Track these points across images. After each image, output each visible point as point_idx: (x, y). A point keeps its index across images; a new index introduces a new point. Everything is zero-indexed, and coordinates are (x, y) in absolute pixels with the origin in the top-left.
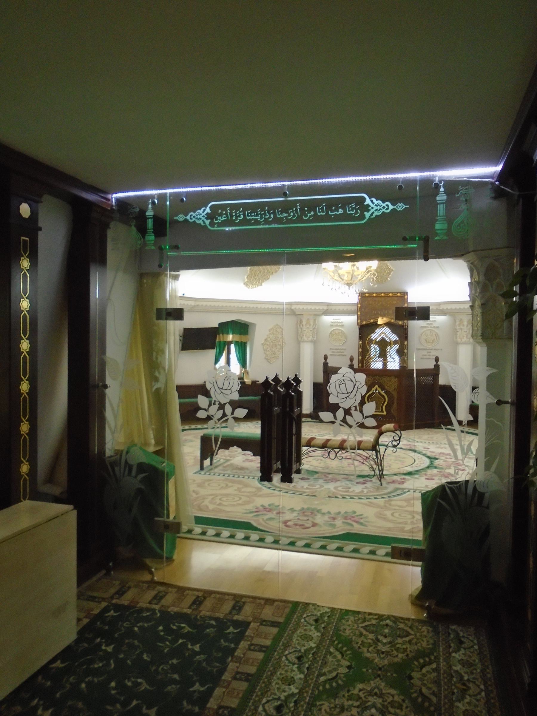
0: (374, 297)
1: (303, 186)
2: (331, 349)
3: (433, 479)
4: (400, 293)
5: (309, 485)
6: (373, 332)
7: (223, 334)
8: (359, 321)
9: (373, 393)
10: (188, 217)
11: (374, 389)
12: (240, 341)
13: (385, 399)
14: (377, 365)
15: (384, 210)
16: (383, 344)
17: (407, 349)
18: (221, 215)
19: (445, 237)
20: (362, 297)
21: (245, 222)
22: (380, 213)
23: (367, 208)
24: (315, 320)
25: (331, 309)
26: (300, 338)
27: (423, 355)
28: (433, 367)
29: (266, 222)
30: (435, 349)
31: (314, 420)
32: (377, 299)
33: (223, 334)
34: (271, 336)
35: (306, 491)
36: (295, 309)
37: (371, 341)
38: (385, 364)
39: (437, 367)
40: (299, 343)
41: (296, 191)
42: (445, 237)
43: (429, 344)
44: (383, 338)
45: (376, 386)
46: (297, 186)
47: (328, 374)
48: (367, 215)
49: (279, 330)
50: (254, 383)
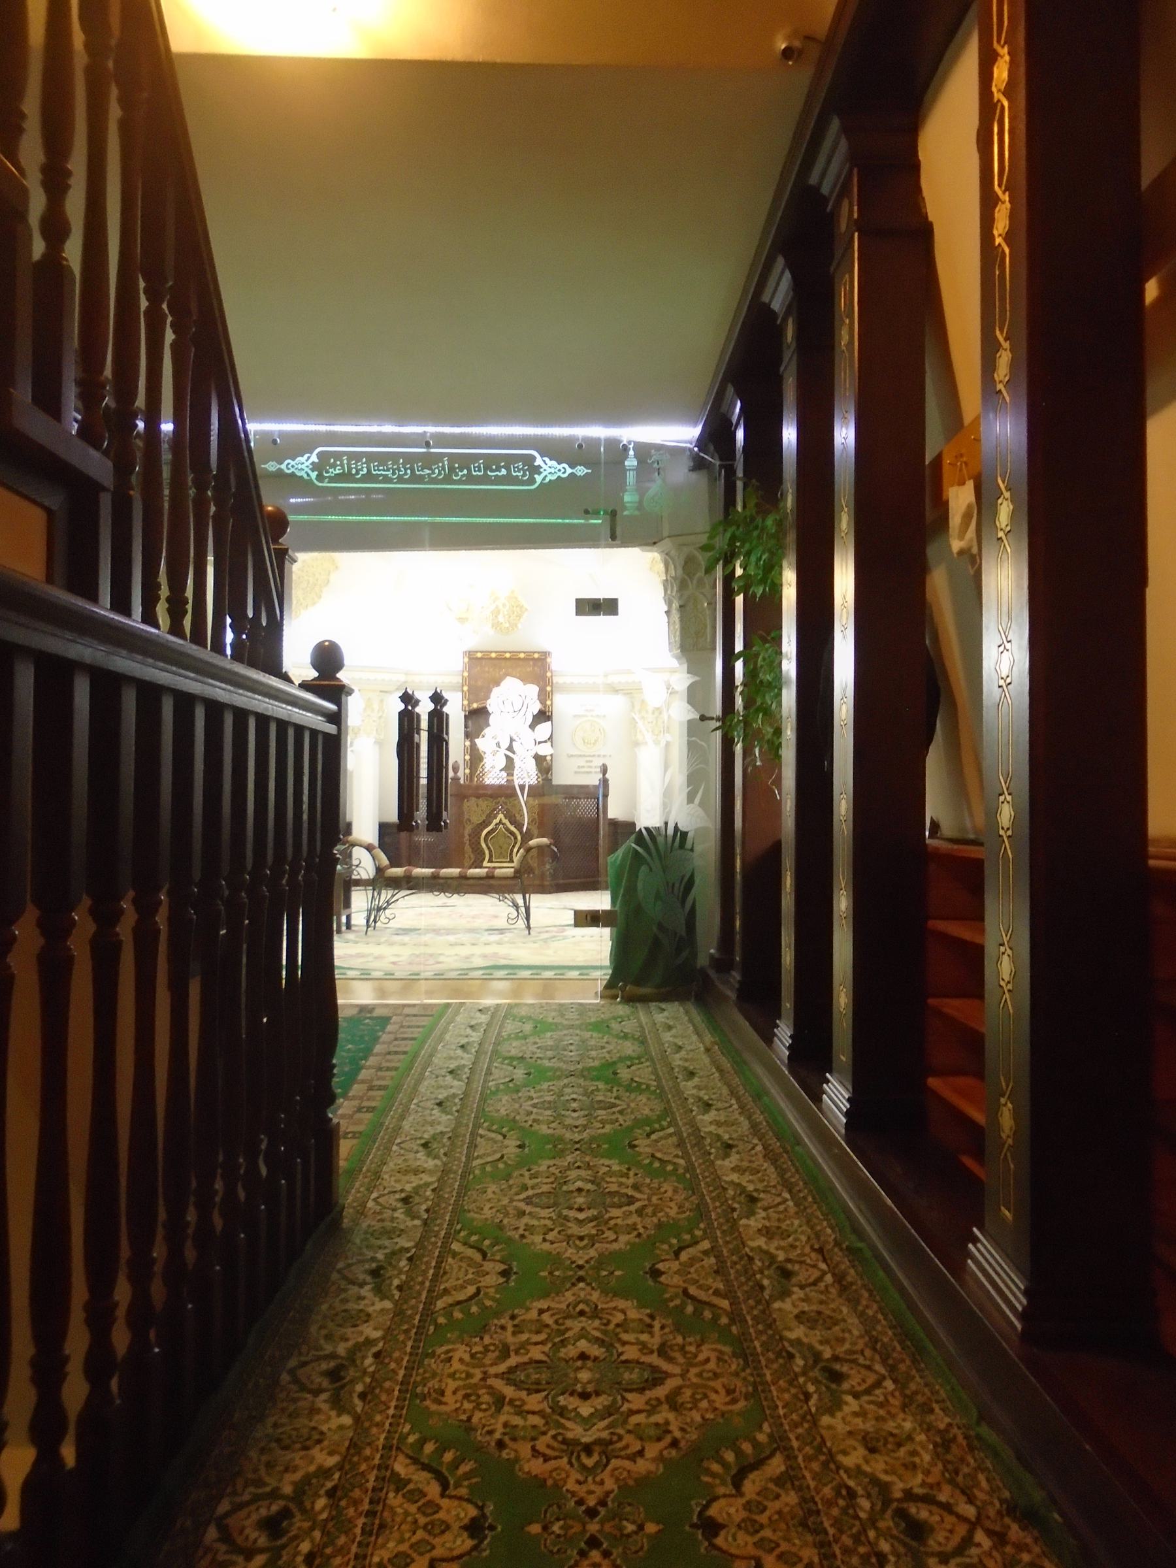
1: (453, 436)
8: (466, 702)
10: (283, 466)
13: (516, 838)
15: (560, 474)
18: (334, 466)
19: (637, 513)
21: (369, 477)
22: (554, 477)
23: (537, 470)
24: (382, 701)
29: (401, 480)
39: (605, 782)
41: (443, 440)
42: (637, 513)
46: (443, 435)
48: (538, 478)
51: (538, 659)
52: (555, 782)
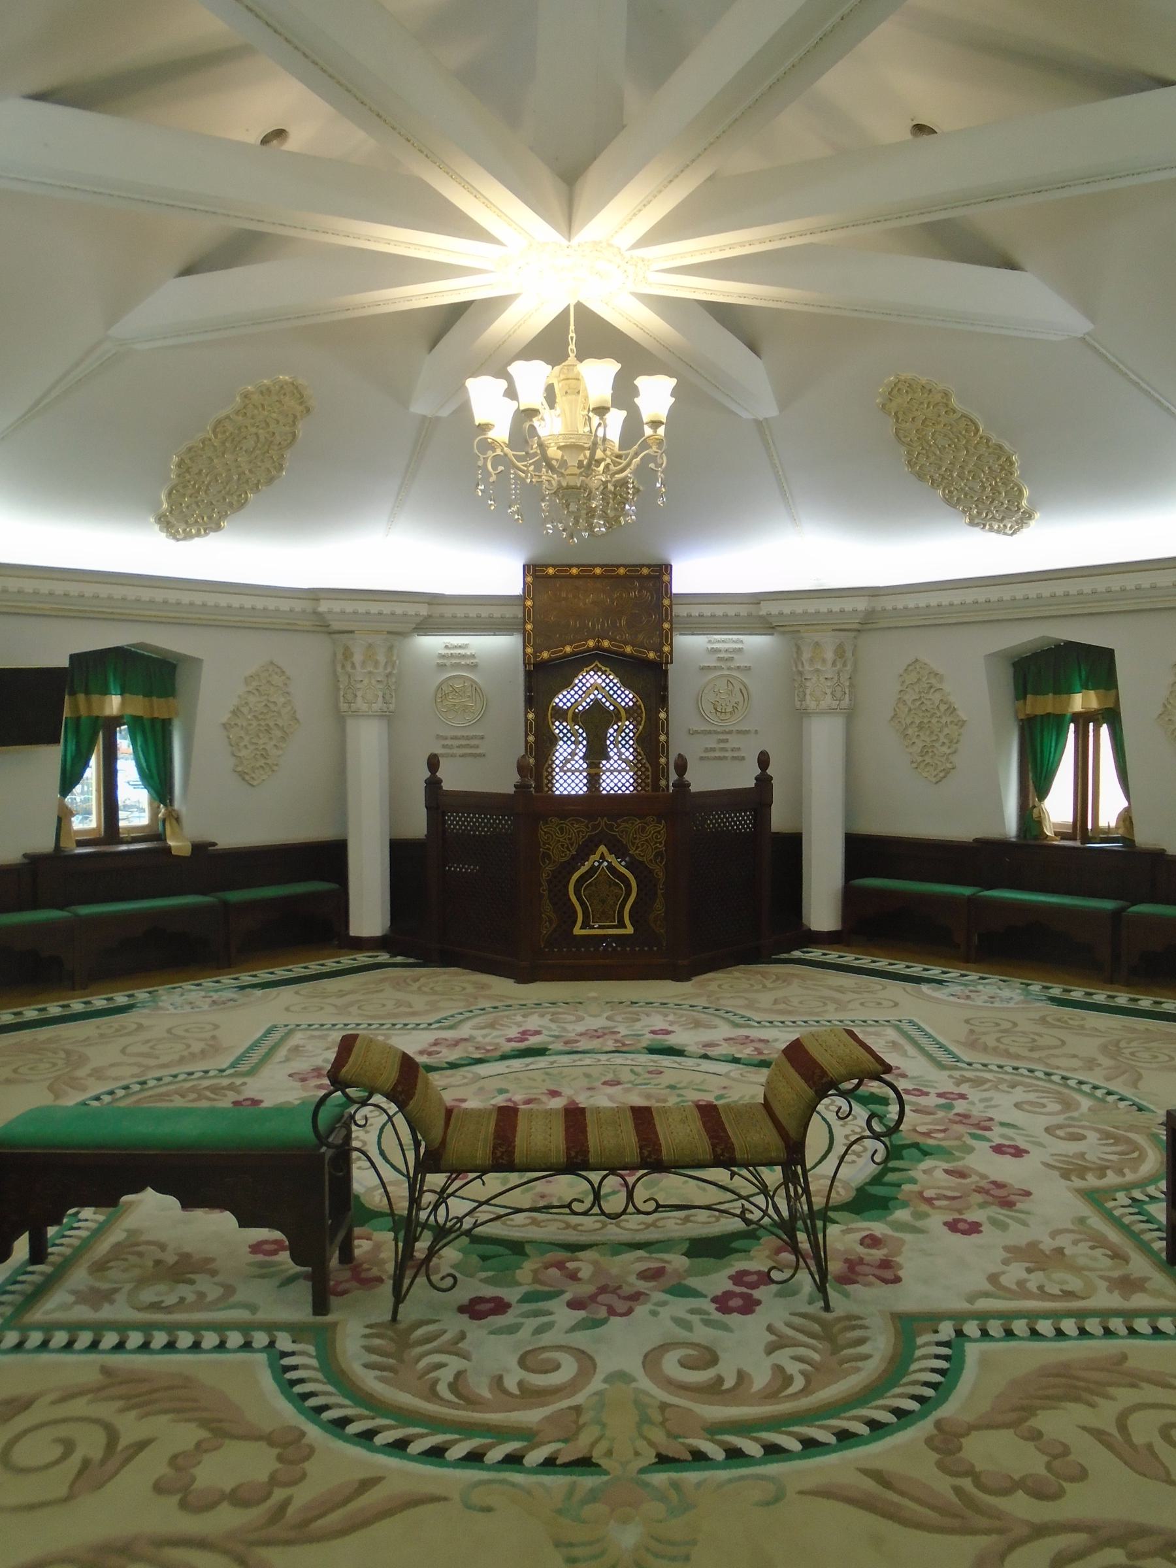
0: (571, 577)
2: (438, 737)
3: (974, 1228)
4: (649, 566)
5: (522, 1362)
6: (567, 683)
7: (87, 692)
8: (529, 650)
9: (593, 870)
11: (594, 859)
12: (147, 716)
14: (569, 782)
16: (595, 721)
17: (667, 734)
20: (535, 577)
24: (391, 648)
25: (442, 616)
26: (343, 706)
27: (707, 750)
28: (751, 783)
30: (738, 732)
31: (399, 959)
32: (580, 582)
33: (87, 692)
34: (252, 699)
35: (532, 1416)
36: (330, 612)
37: (560, 714)
38: (593, 780)
39: (764, 782)
40: (340, 719)
43: (723, 717)
44: (597, 702)
45: (602, 849)
47: (444, 814)
49: (277, 680)
50: (200, 849)
51: (648, 577)
52: (693, 789)
